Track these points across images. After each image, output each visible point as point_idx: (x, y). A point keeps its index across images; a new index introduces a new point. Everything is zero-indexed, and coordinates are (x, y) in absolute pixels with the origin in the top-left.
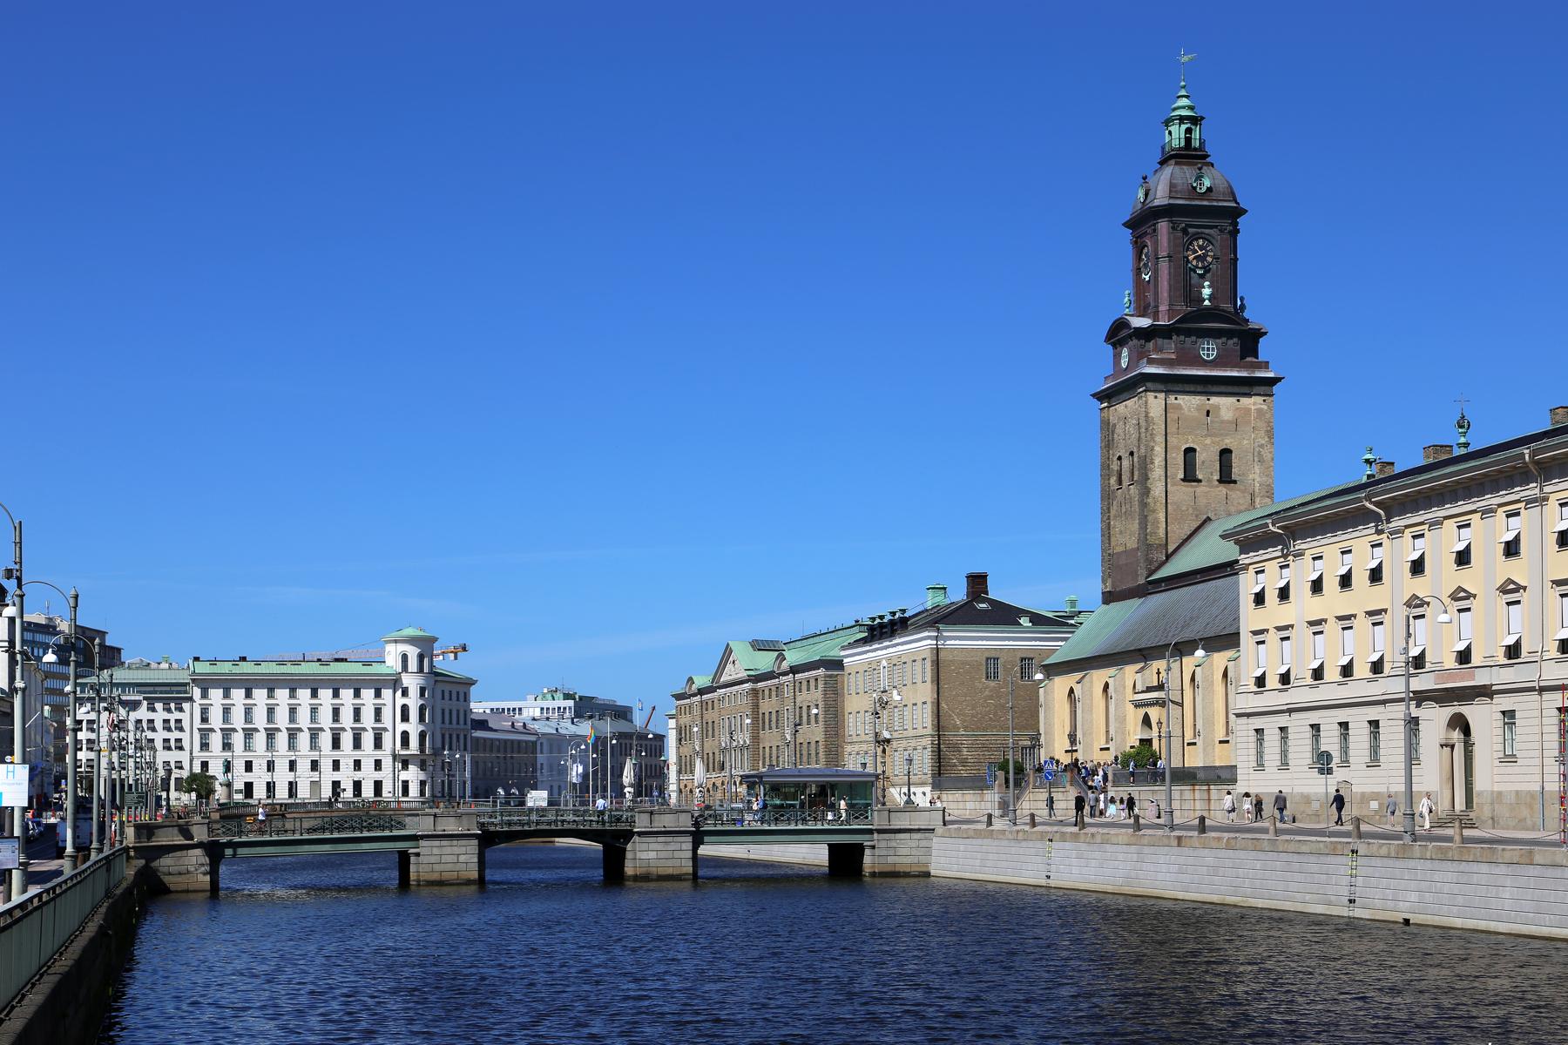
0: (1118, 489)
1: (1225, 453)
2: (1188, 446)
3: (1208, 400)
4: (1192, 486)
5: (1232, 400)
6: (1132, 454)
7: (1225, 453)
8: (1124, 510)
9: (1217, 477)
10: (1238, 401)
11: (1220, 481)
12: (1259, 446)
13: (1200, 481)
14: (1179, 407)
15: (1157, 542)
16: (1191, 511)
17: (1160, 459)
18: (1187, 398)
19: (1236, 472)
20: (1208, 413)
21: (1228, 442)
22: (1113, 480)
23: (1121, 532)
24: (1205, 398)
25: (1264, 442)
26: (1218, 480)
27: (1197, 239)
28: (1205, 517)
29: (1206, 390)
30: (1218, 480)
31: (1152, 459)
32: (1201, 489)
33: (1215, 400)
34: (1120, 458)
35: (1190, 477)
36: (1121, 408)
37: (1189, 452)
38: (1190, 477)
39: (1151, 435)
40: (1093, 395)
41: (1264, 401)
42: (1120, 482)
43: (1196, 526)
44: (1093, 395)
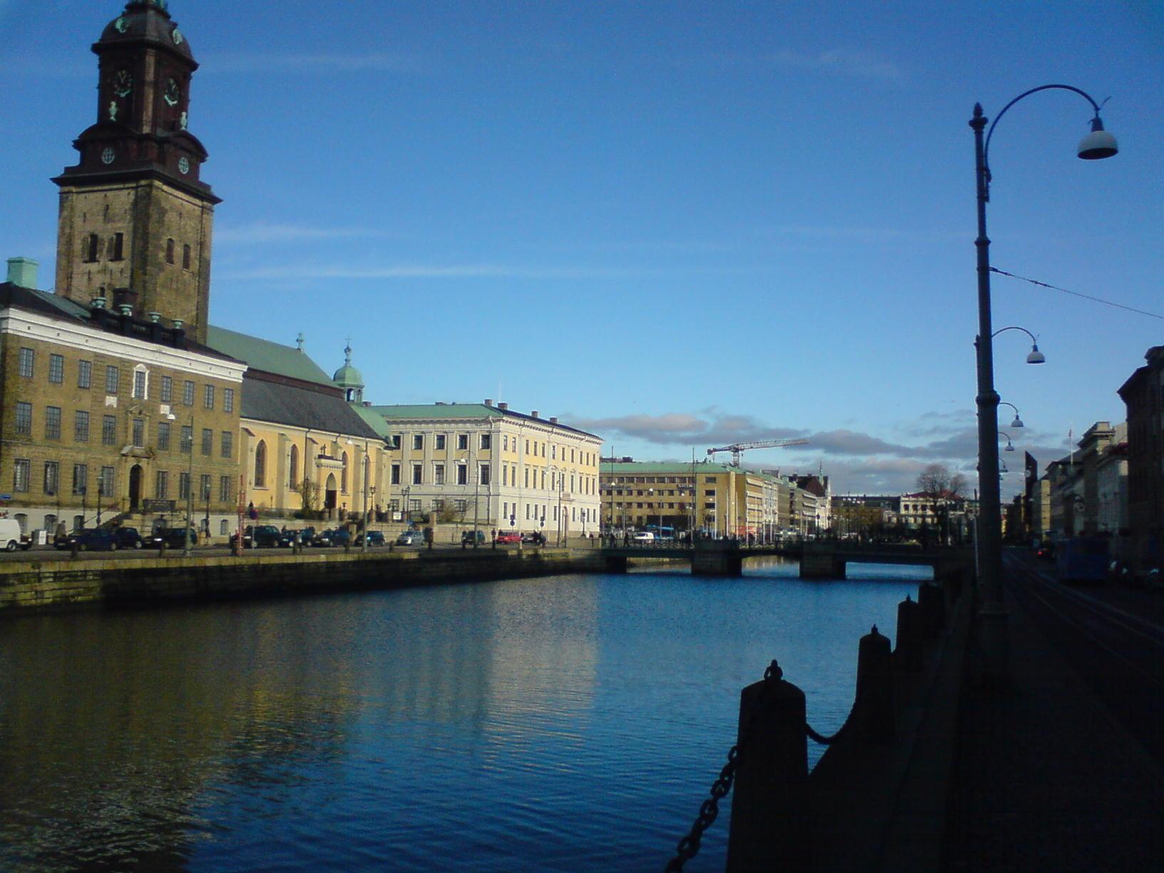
8: (174, 286)
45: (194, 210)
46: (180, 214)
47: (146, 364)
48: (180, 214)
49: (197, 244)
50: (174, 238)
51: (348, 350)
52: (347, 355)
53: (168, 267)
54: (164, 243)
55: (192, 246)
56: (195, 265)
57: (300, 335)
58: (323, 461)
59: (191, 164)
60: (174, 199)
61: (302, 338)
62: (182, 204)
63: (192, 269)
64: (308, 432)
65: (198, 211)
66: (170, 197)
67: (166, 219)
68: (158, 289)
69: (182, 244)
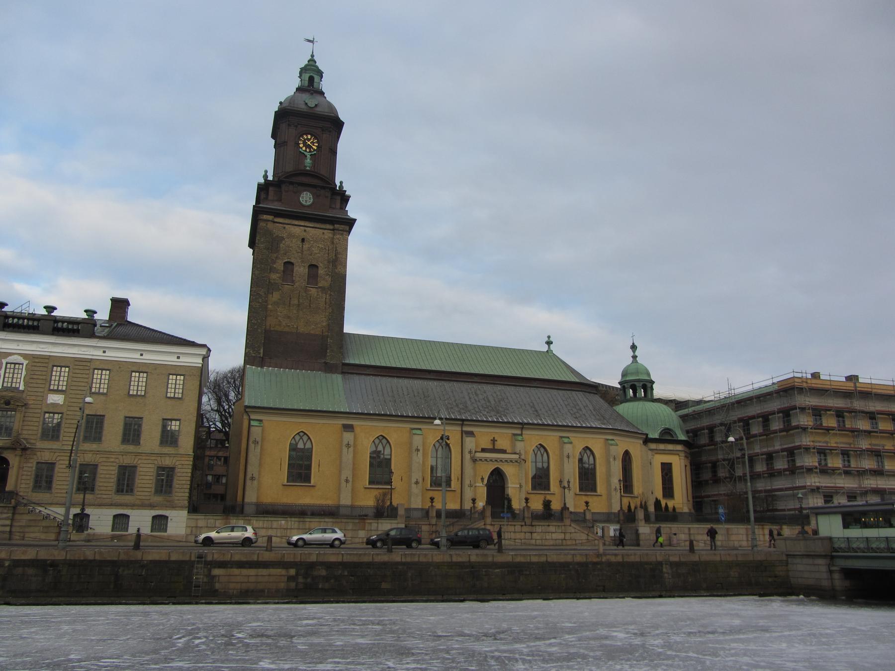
45: (323, 233)
46: (303, 240)
47: (25, 356)
48: (303, 240)
49: (329, 262)
50: (292, 261)
51: (634, 347)
52: (634, 352)
53: (287, 288)
54: (279, 265)
55: (321, 265)
56: (325, 282)
57: (549, 337)
58: (479, 455)
59: (316, 196)
60: (297, 229)
61: (551, 339)
62: (305, 231)
63: (320, 285)
64: (462, 425)
65: (328, 234)
66: (287, 226)
67: (282, 245)
68: (270, 306)
69: (307, 265)
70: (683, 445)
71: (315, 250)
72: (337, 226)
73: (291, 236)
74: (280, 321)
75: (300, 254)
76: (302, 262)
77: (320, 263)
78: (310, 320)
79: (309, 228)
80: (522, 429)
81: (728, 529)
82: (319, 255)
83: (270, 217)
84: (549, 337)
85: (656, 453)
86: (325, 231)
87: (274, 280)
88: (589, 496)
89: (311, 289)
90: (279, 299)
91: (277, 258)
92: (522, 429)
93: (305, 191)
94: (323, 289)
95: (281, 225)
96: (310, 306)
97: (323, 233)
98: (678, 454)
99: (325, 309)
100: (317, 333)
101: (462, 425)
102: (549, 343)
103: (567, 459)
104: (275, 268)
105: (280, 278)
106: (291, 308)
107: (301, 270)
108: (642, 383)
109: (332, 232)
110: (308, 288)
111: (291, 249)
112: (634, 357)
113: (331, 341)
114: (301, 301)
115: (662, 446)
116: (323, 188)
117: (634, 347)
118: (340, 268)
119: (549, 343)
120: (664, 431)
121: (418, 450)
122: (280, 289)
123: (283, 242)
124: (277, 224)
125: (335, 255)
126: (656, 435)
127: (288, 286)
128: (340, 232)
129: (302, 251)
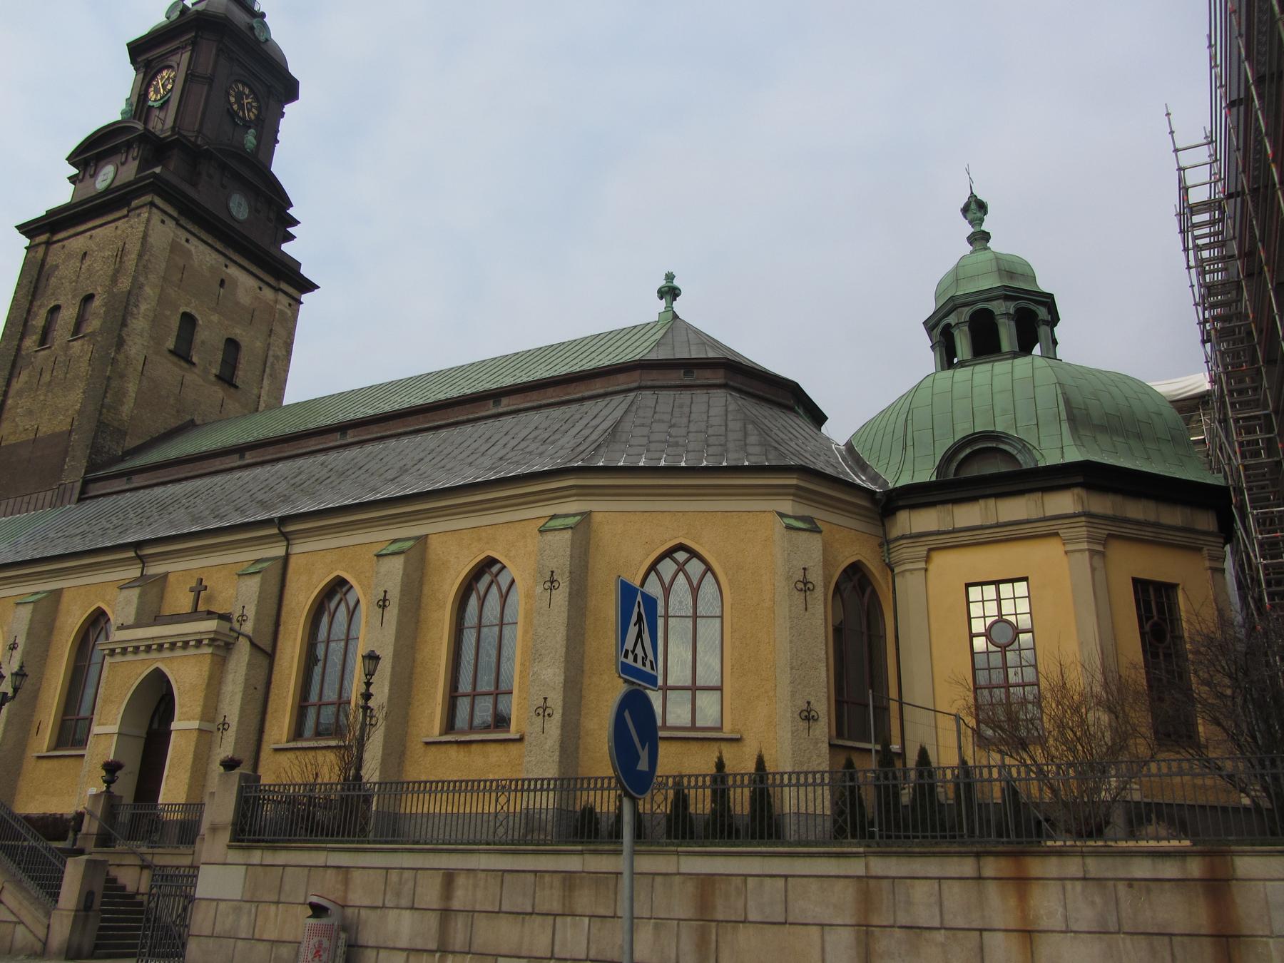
0: (36, 351)
1: (232, 346)
2: (188, 310)
3: (226, 266)
4: (181, 367)
5: (251, 282)
6: (89, 298)
7: (232, 346)
8: (46, 377)
9: (215, 371)
10: (260, 289)
11: (218, 377)
12: (273, 356)
13: (194, 364)
14: (188, 254)
15: (116, 424)
16: (172, 401)
17: (149, 306)
18: (202, 247)
19: (241, 375)
20: (222, 283)
21: (238, 332)
22: (30, 342)
23: (30, 412)
24: (222, 260)
25: (279, 354)
26: (216, 376)
27: (244, 84)
28: (189, 418)
29: (227, 253)
30: (216, 376)
31: (139, 301)
32: (192, 377)
33: (233, 271)
34: (57, 308)
35: (182, 353)
36: (78, 244)
37: (188, 321)
38: (182, 353)
39: (145, 267)
40: (18, 227)
41: (290, 305)
42: (44, 340)
43: (174, 425)
44: (18, 227)
46: (85, 254)
57: (670, 277)
61: (676, 283)
63: (88, 328)
70: (1077, 491)
71: (97, 266)
72: (135, 203)
73: (69, 256)
74: (17, 426)
75: (74, 284)
76: (74, 297)
77: (99, 289)
78: (60, 405)
79: (97, 230)
80: (287, 537)
81: (707, 883)
82: (101, 272)
83: (43, 238)
84: (670, 277)
85: (930, 550)
86: (119, 223)
87: (27, 349)
88: (474, 747)
89: (75, 343)
90: (26, 382)
91: (40, 307)
92: (287, 537)
93: (103, 166)
94: (93, 334)
95: (60, 244)
96: (65, 378)
97: (116, 228)
98: (1057, 534)
99: (87, 374)
100: (64, 429)
101: (142, 560)
102: (670, 292)
103: (381, 610)
104: (33, 325)
105: (34, 342)
106: (39, 392)
107: (68, 314)
108: (966, 313)
109: (126, 219)
110: (71, 343)
111: (63, 281)
112: (980, 239)
113: (76, 437)
114: (55, 373)
115: (968, 515)
116: (128, 145)
117: (975, 208)
118: (122, 283)
119: (670, 292)
120: (968, 451)
121: (13, 647)
122: (32, 363)
123: (56, 273)
124: (55, 246)
125: (120, 262)
126: (926, 474)
127: (42, 353)
128: (138, 211)
129: (78, 277)
